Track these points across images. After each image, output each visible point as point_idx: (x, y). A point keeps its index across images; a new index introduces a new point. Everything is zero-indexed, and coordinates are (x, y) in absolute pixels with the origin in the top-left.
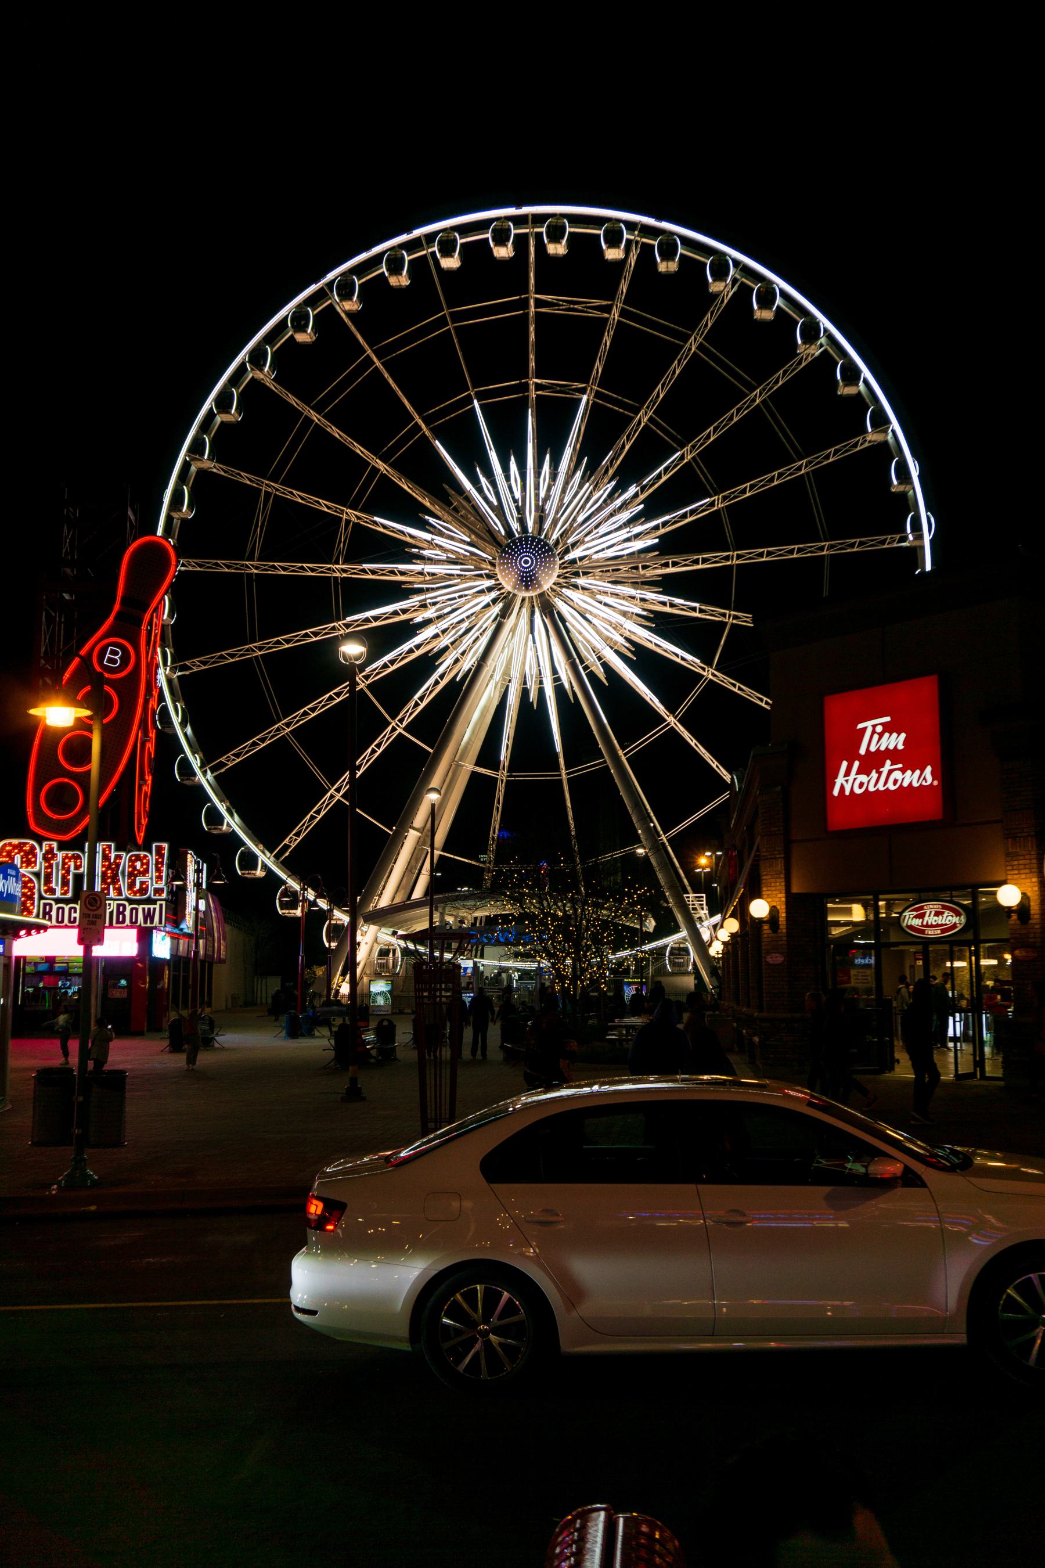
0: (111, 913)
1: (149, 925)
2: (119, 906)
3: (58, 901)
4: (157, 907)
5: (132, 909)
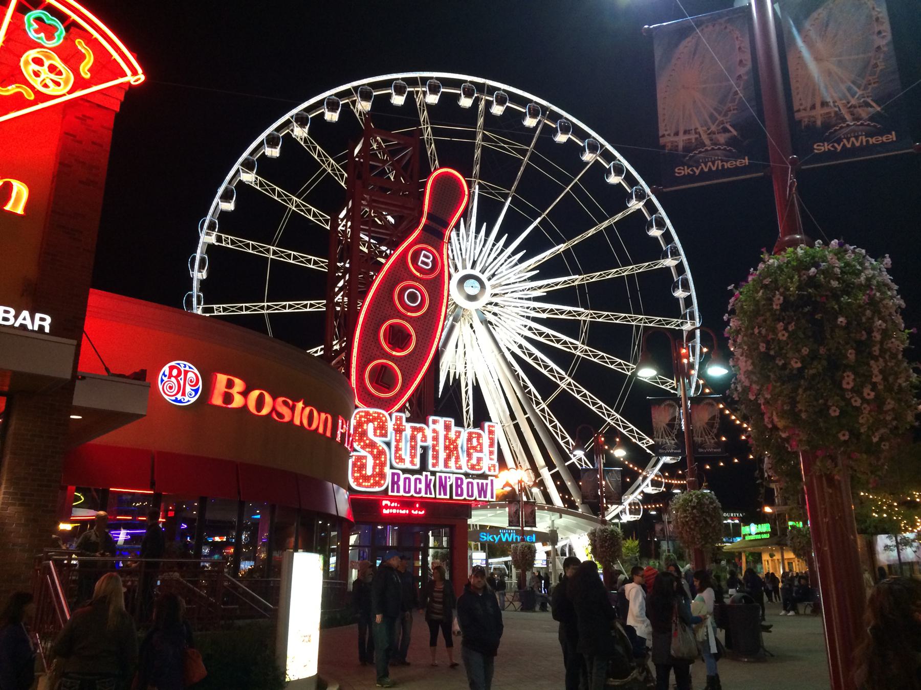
0: (451, 486)
1: (482, 499)
2: (457, 479)
3: (405, 471)
4: (489, 481)
5: (468, 483)
